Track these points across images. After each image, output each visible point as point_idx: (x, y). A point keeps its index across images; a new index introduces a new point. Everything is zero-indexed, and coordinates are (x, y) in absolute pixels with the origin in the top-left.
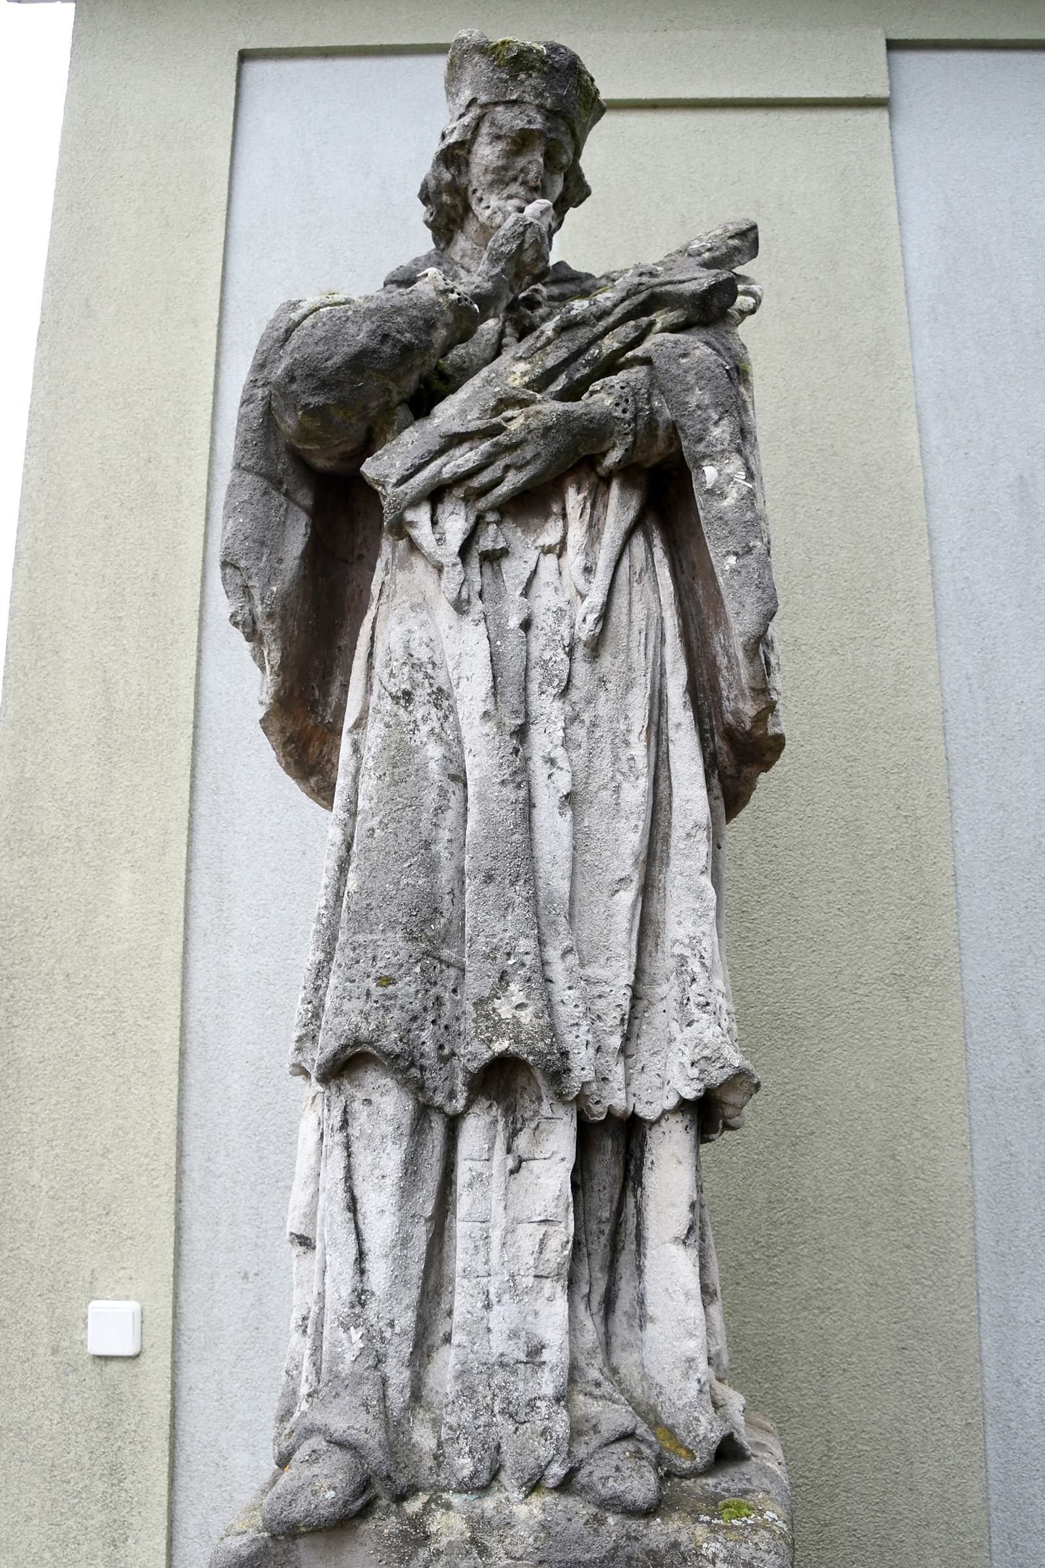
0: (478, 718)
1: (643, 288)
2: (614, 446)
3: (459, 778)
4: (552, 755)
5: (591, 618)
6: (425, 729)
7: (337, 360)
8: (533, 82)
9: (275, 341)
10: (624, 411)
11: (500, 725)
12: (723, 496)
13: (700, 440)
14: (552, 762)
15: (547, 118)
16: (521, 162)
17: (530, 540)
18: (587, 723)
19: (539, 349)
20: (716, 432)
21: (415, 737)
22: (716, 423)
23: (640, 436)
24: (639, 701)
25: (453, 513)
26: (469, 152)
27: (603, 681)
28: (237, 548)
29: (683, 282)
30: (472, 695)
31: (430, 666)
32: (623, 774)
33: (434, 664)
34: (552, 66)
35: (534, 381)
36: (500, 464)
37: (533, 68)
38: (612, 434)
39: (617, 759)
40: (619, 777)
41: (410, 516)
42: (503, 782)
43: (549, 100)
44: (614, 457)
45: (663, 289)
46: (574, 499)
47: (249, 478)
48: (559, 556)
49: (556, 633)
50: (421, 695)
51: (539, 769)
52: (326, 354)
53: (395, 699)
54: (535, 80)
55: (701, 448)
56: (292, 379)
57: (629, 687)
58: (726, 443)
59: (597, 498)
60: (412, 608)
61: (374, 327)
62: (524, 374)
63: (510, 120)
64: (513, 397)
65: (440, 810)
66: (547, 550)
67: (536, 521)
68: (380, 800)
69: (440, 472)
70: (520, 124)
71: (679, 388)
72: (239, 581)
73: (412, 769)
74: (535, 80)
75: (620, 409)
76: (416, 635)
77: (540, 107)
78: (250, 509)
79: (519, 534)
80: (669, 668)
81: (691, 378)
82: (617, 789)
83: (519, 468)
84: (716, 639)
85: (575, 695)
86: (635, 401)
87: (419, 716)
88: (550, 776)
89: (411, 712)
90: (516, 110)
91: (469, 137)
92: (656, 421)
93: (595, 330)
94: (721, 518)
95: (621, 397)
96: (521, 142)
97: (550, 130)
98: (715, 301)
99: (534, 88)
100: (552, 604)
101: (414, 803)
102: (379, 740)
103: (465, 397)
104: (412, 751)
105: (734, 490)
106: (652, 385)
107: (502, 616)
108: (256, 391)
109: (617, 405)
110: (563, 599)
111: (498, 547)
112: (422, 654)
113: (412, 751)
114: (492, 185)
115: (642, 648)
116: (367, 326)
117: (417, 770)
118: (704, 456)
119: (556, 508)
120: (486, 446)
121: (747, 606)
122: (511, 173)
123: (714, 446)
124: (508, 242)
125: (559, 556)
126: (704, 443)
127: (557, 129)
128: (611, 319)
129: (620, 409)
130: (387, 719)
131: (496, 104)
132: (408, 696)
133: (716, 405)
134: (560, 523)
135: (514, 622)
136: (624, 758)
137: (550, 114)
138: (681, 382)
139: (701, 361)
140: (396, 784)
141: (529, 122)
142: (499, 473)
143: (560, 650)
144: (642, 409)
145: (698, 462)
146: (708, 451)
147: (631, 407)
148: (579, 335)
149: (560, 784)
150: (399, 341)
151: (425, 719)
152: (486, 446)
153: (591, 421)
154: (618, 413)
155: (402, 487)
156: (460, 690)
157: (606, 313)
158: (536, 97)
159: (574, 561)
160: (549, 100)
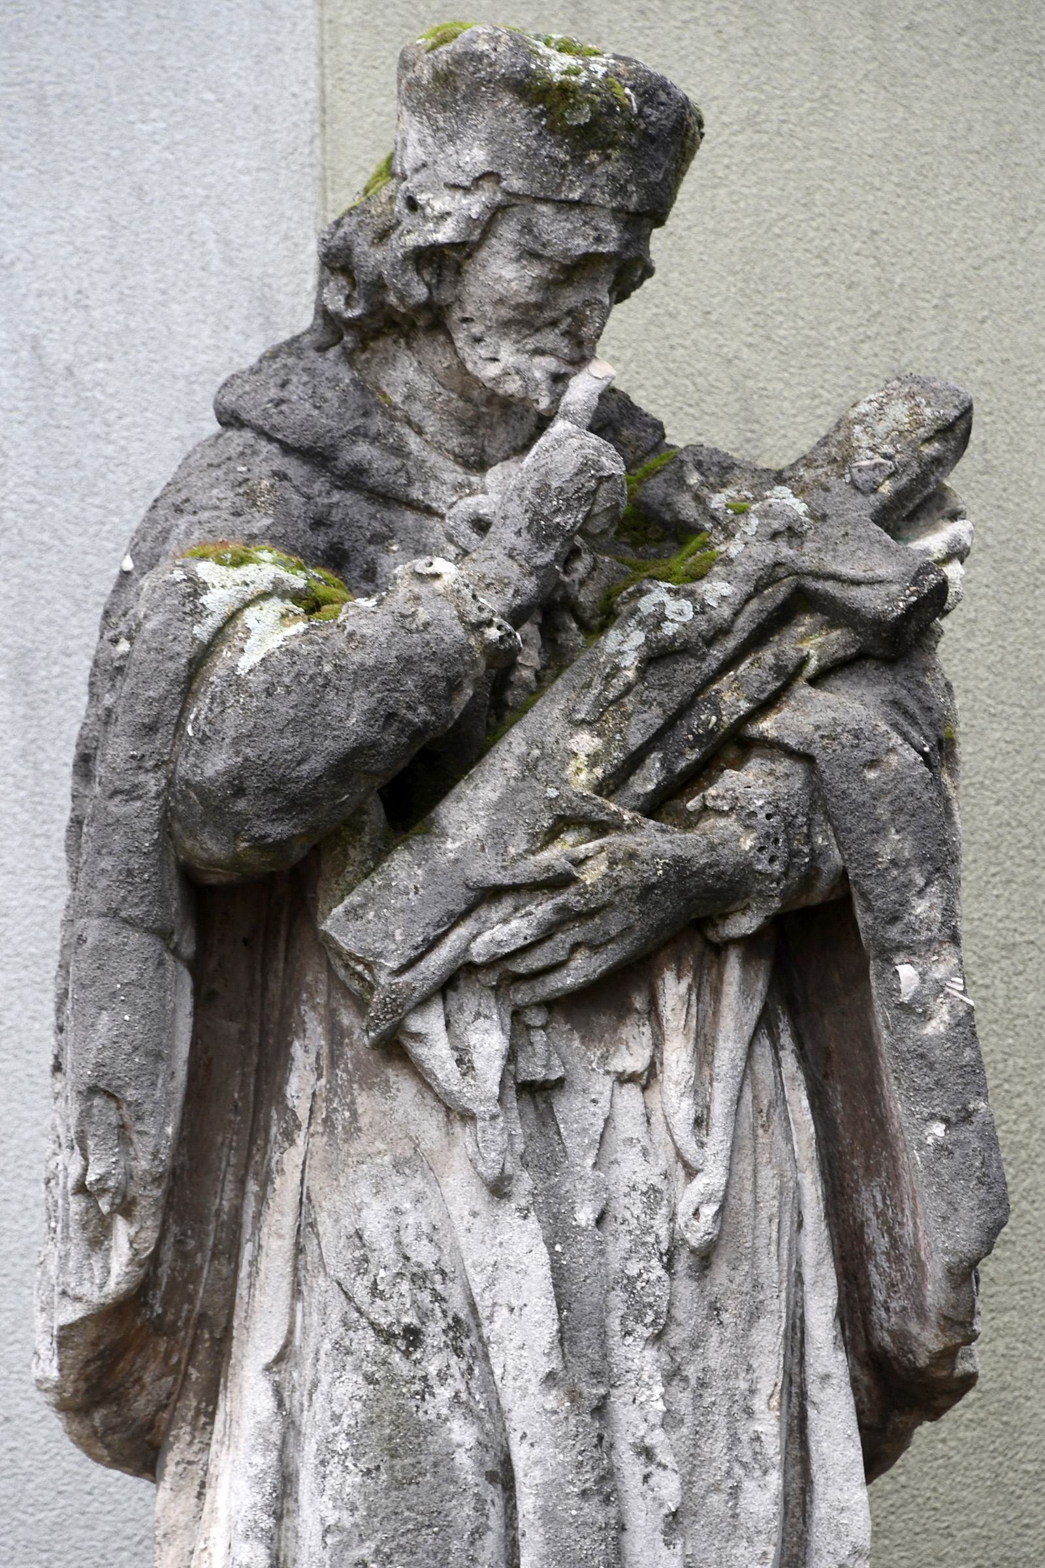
0: (535, 1381)
1: (781, 571)
3: (503, 1476)
4: (648, 1442)
5: (709, 1211)
6: (444, 1393)
7: (316, 764)
9: (173, 683)
10: (772, 860)
11: (574, 1396)
12: (926, 1016)
13: (894, 919)
14: (647, 1453)
17: (595, 1053)
18: (693, 1382)
20: (921, 907)
21: (425, 1406)
22: (921, 893)
24: (769, 1336)
25: (478, 1015)
27: (715, 1309)
28: (121, 1065)
29: (857, 583)
30: (523, 1337)
31: (438, 1277)
32: (744, 1465)
33: (443, 1273)
36: (565, 939)
39: (735, 1440)
40: (738, 1471)
41: (416, 1024)
42: (584, 1494)
44: (745, 924)
45: (820, 585)
46: (673, 990)
47: (135, 938)
48: (644, 1089)
49: (648, 1230)
50: (435, 1332)
51: (631, 1468)
52: (298, 753)
53: (386, 1336)
56: (240, 792)
57: (754, 1315)
59: (707, 989)
60: (397, 1166)
61: (372, 702)
62: (594, 760)
65: (478, 1533)
66: (623, 1079)
67: (604, 1020)
68: (371, 1513)
69: (467, 950)
72: (114, 1119)
73: (427, 1462)
75: (765, 856)
76: (410, 1219)
78: (141, 998)
79: (576, 1043)
80: (808, 1274)
81: (883, 811)
82: (735, 1492)
83: (594, 947)
84: (865, 1195)
85: (676, 1336)
86: (788, 840)
87: (432, 1370)
88: (646, 1478)
89: (417, 1362)
94: (922, 1056)
100: (639, 1178)
101: (436, 1519)
102: (358, 1406)
103: (494, 796)
104: (425, 1430)
105: (945, 1009)
106: (813, 806)
107: (561, 1200)
108: (142, 777)
109: (761, 849)
110: (658, 1170)
111: (553, 1077)
112: (424, 1254)
113: (425, 1430)
115: (773, 1248)
116: (362, 701)
117: (435, 1465)
119: (639, 1002)
120: (543, 909)
121: (962, 1212)
124: (569, 508)
125: (644, 1089)
128: (731, 643)
129: (765, 856)
130: (368, 1368)
132: (413, 1336)
133: (922, 860)
134: (647, 1030)
135: (585, 1215)
136: (745, 1438)
139: (899, 777)
140: (399, 1486)
142: (561, 955)
143: (655, 1262)
145: (887, 953)
146: (906, 940)
148: (679, 676)
149: (664, 1493)
150: (410, 723)
151: (443, 1377)
152: (543, 909)
153: (718, 877)
155: (406, 977)
156: (496, 1326)
157: (723, 631)
159: (683, 1108)
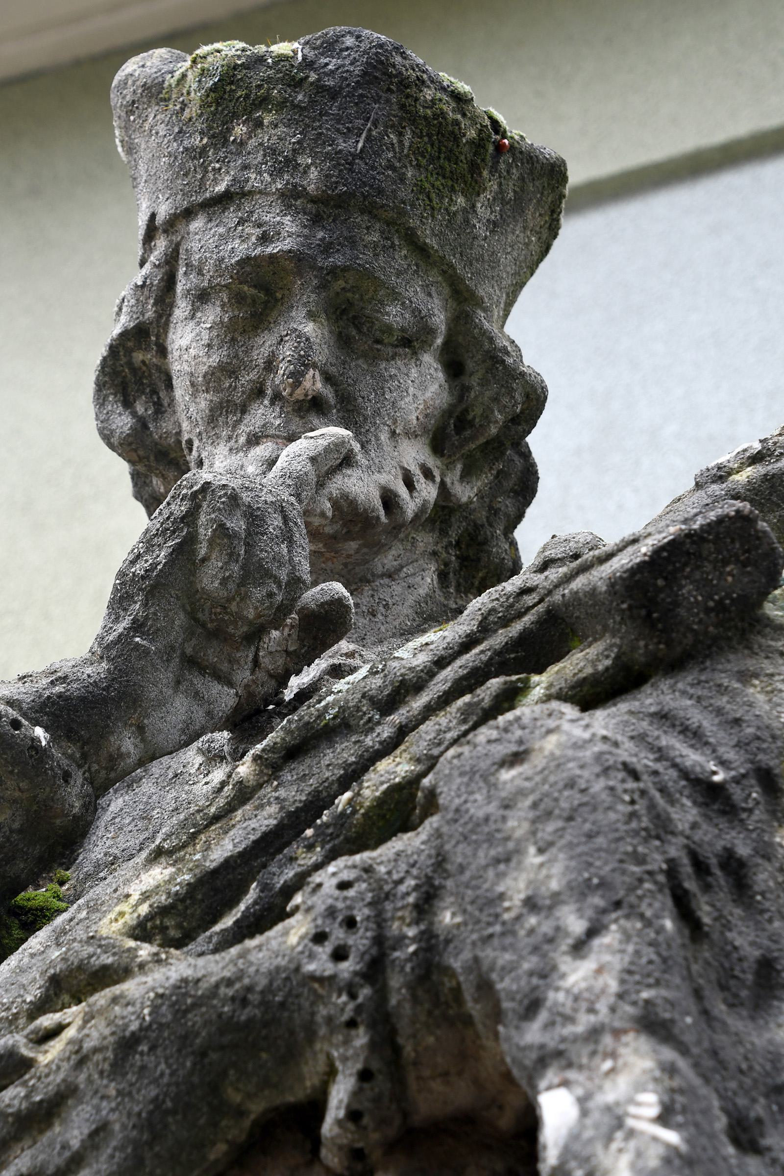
1: (529, 600)
2: (331, 1073)
8: (264, 137)
10: (339, 955)
15: (316, 220)
16: (264, 345)
19: (216, 818)
20: (577, 974)
22: (579, 948)
23: (404, 1027)
26: (163, 351)
34: (319, 88)
35: (163, 911)
37: (263, 102)
38: (311, 1035)
43: (313, 174)
54: (275, 131)
55: (533, 1034)
58: (602, 1007)
63: (214, 243)
64: (81, 967)
70: (239, 249)
71: (483, 856)
74: (275, 131)
75: (324, 951)
77: (290, 197)
81: (517, 824)
90: (231, 217)
91: (150, 314)
92: (448, 971)
93: (369, 741)
95: (331, 912)
96: (255, 295)
97: (326, 248)
98: (687, 589)
99: (272, 151)
114: (212, 419)
118: (546, 1058)
122: (247, 378)
123: (569, 1019)
126: (543, 1016)
127: (353, 242)
131: (188, 214)
133: (581, 890)
137: (321, 209)
138: (490, 839)
141: (264, 239)
144: (400, 941)
146: (551, 1040)
147: (360, 941)
153: (243, 1001)
154: (320, 963)
158: (276, 173)
160: (313, 174)
